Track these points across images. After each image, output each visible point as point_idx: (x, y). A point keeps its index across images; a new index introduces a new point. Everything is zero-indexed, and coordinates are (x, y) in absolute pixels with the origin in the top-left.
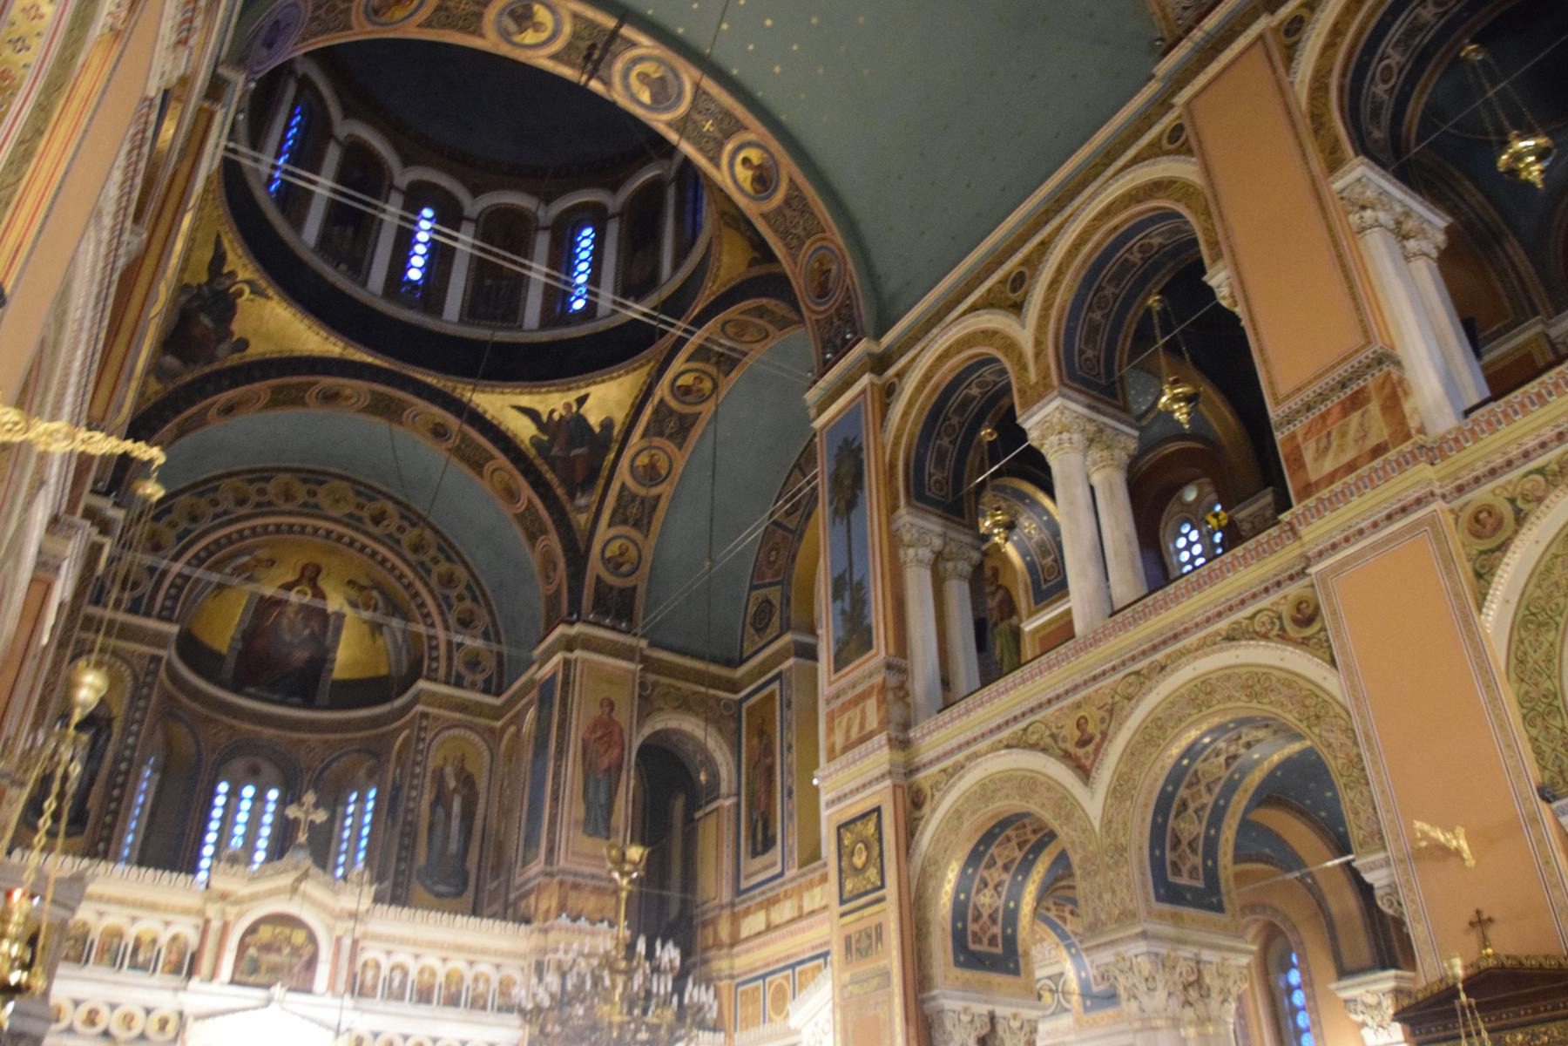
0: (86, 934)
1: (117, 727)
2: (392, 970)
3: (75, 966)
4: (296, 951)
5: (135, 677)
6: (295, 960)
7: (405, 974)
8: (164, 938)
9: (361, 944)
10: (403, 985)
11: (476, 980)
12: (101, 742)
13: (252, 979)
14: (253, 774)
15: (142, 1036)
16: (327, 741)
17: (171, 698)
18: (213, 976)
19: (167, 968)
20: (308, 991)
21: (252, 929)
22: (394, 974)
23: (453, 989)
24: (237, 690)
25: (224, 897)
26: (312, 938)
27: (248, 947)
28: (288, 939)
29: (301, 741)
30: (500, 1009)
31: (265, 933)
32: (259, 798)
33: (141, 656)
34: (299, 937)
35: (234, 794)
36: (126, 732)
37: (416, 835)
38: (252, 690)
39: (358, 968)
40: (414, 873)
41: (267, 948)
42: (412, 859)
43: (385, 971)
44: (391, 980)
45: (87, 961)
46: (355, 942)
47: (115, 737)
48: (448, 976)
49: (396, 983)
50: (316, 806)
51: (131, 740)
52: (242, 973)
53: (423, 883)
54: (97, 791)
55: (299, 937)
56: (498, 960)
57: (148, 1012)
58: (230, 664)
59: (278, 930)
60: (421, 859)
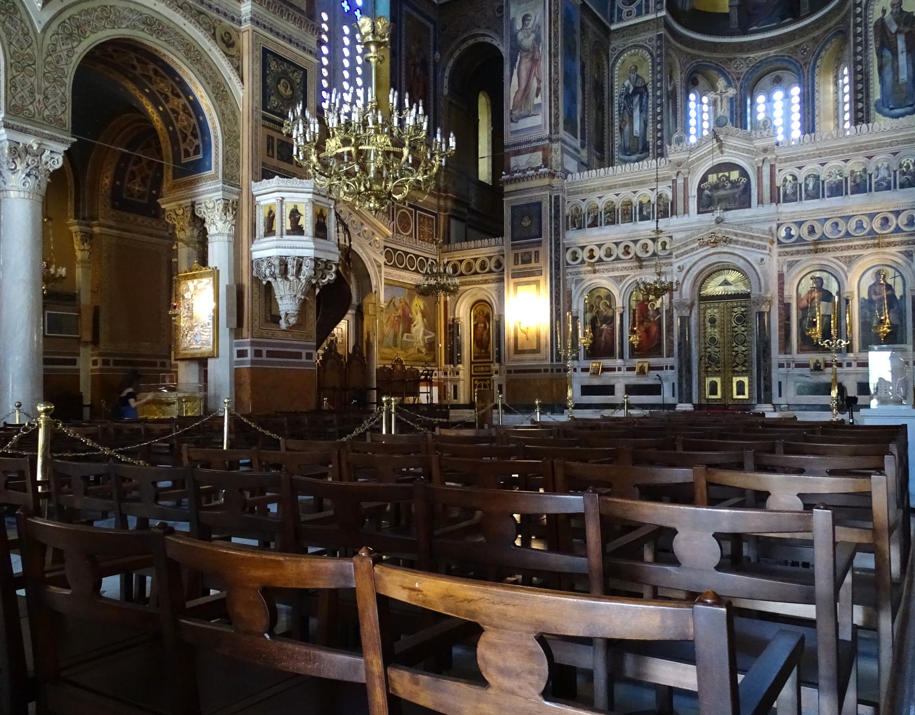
0: (614, 209)
1: (650, 87)
2: (806, 179)
3: (613, 226)
4: (734, 184)
5: (651, 54)
6: (736, 190)
7: (817, 178)
8: (653, 198)
9: (778, 166)
10: (816, 186)
11: (878, 169)
12: (644, 100)
13: (710, 209)
14: (778, 81)
15: (654, 254)
16: (814, 38)
17: (693, 57)
18: (686, 211)
19: (659, 215)
20: (749, 206)
21: (704, 179)
22: (807, 182)
23: (858, 181)
24: (745, 33)
25: (679, 164)
26: (744, 173)
27: (704, 189)
28: (728, 178)
29: (797, 46)
30: (902, 186)
31: (712, 178)
32: (787, 96)
33: (651, 40)
34: (735, 175)
35: (769, 100)
36: (655, 89)
37: (868, 80)
38: (755, 28)
39: (779, 182)
40: (872, 108)
41: (715, 187)
42: (868, 96)
43: (801, 180)
44: (807, 185)
45: (618, 223)
46: (772, 167)
47: (650, 94)
48: (852, 172)
49: (811, 187)
50: (726, 87)
51: (658, 93)
52: (704, 207)
53: (880, 112)
54: (650, 128)
55: (735, 175)
56: (894, 149)
57: (654, 240)
58: (735, 18)
59: (720, 175)
60: (876, 93)
